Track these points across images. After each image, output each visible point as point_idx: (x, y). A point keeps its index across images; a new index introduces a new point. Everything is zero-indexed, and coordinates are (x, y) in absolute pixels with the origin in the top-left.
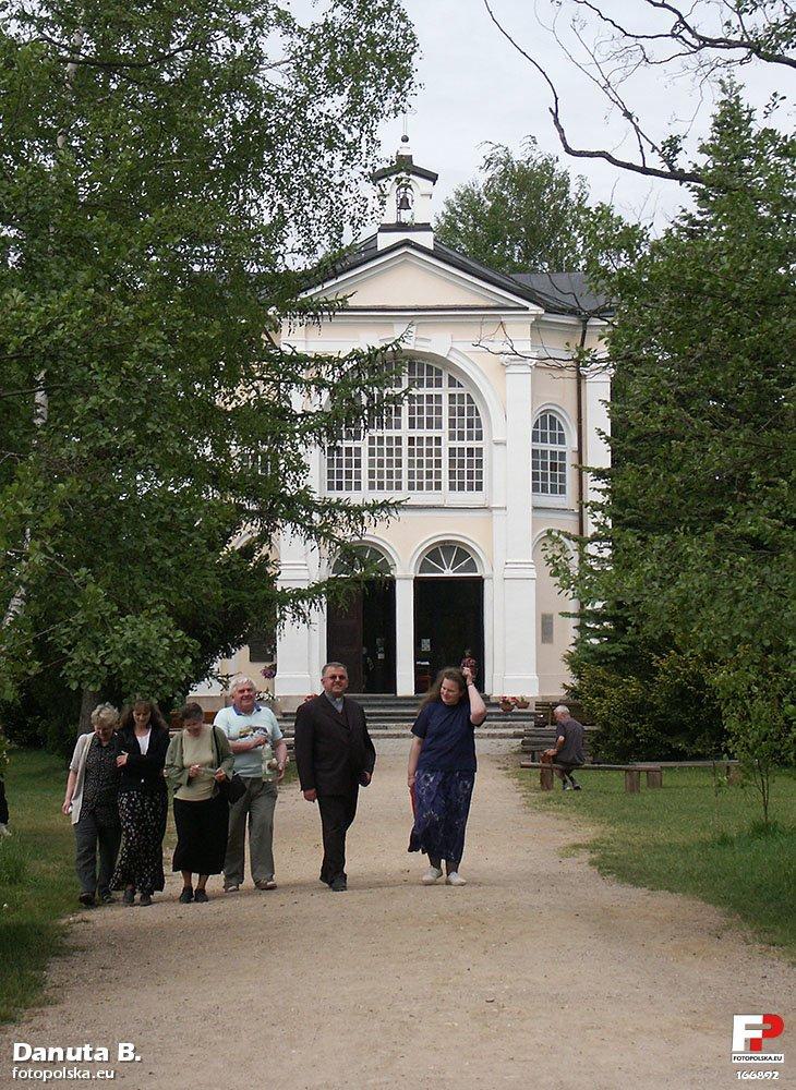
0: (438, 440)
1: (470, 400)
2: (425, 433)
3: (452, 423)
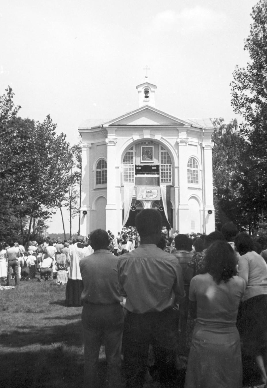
1: (168, 154)
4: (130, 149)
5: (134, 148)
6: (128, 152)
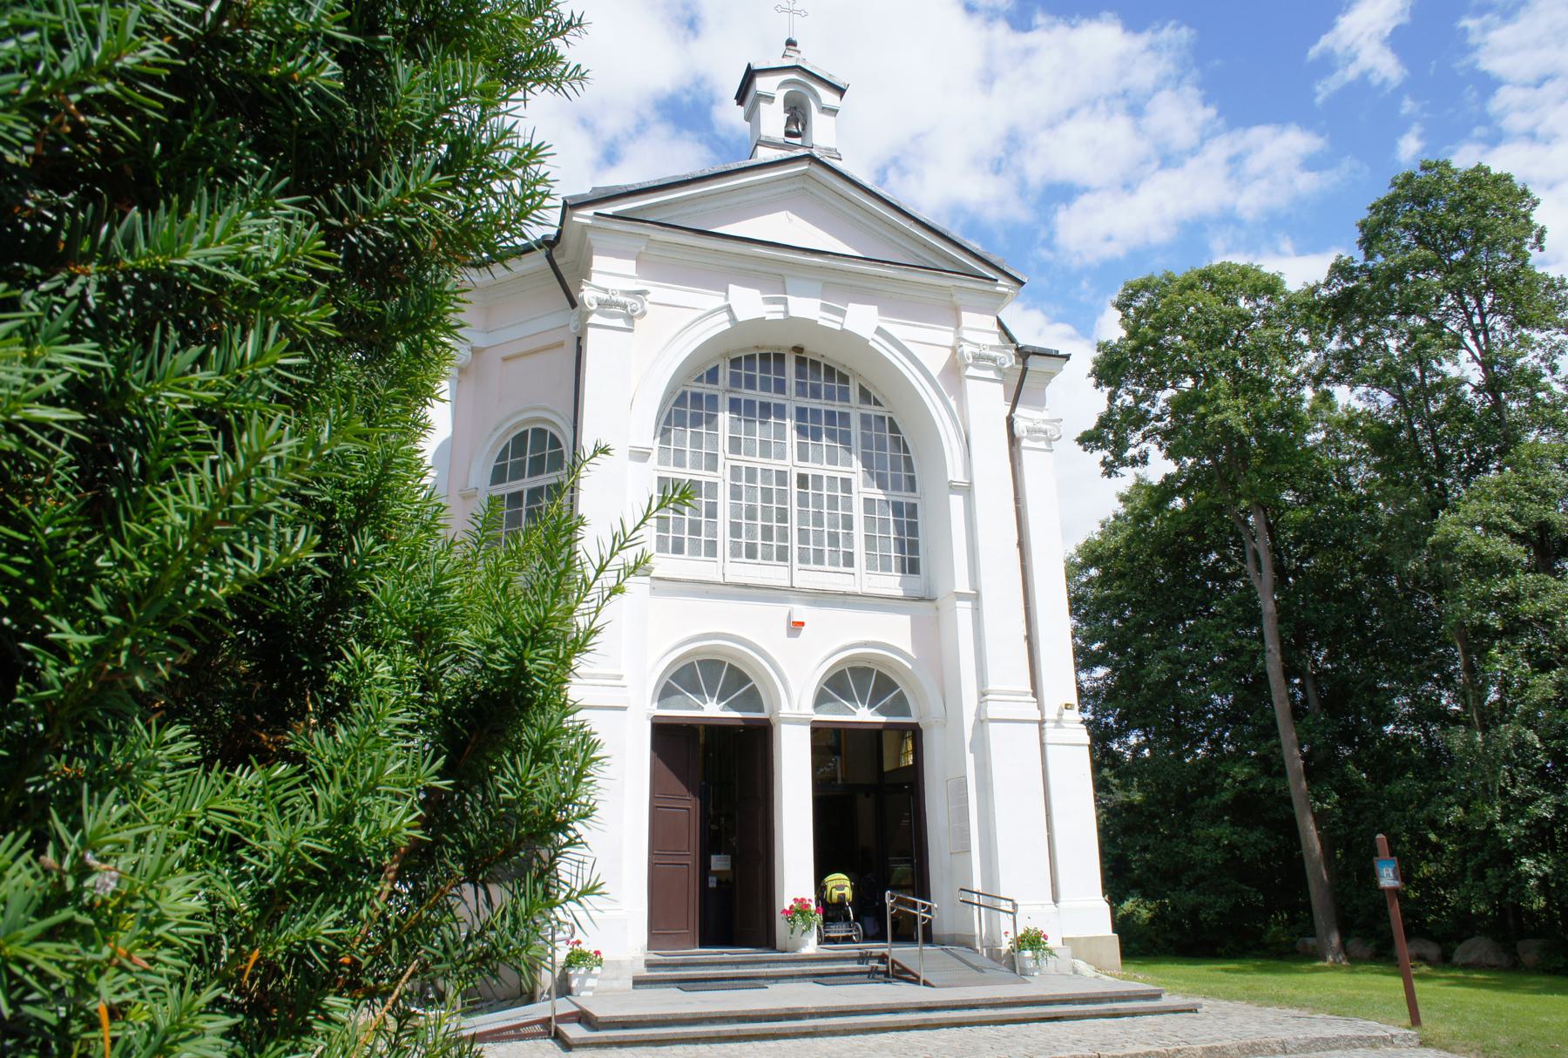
0: (847, 485)
1: (894, 428)
4: (700, 379)
6: (689, 390)
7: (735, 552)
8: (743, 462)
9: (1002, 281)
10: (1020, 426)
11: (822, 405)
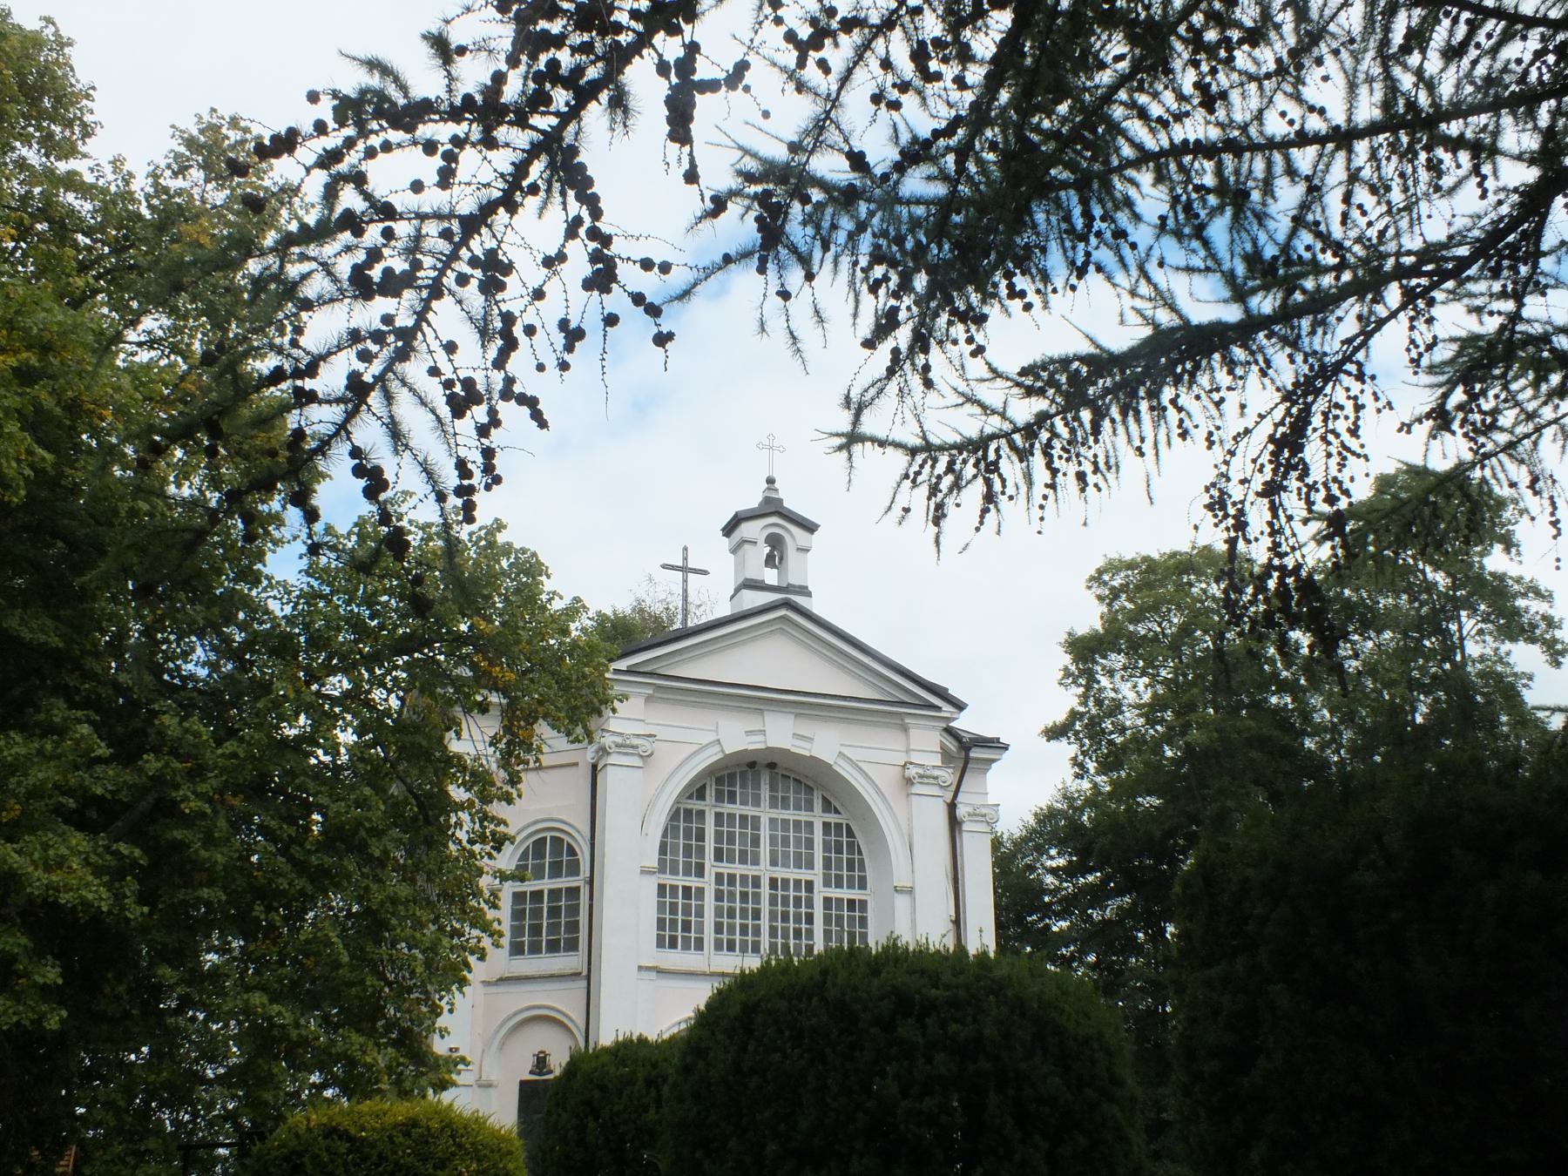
0: (810, 886)
1: (850, 833)
2: (792, 874)
3: (827, 863)
4: (690, 797)
5: (710, 794)
6: (682, 807)
7: (718, 946)
8: (726, 868)
9: (946, 707)
10: (961, 811)
11: (790, 815)
